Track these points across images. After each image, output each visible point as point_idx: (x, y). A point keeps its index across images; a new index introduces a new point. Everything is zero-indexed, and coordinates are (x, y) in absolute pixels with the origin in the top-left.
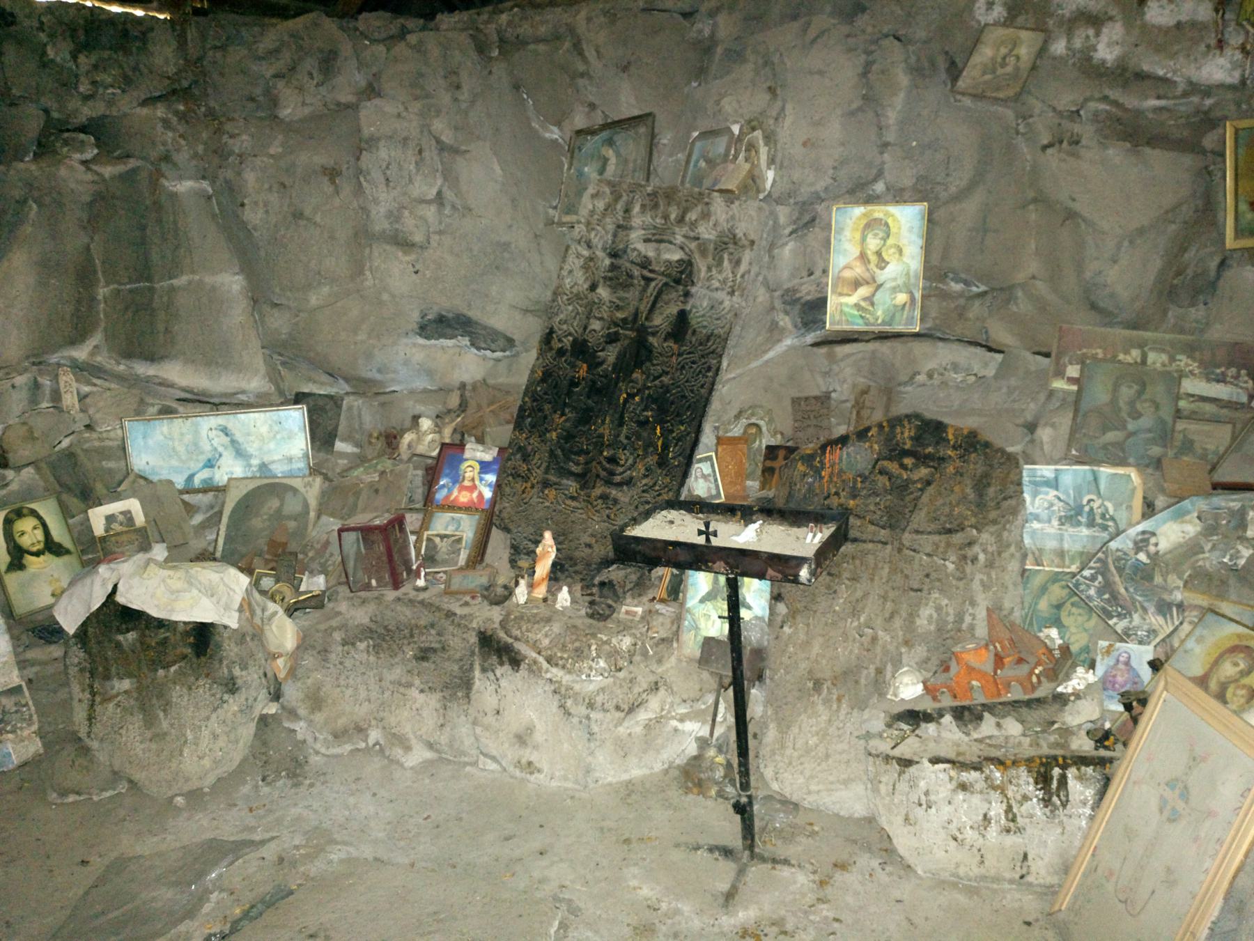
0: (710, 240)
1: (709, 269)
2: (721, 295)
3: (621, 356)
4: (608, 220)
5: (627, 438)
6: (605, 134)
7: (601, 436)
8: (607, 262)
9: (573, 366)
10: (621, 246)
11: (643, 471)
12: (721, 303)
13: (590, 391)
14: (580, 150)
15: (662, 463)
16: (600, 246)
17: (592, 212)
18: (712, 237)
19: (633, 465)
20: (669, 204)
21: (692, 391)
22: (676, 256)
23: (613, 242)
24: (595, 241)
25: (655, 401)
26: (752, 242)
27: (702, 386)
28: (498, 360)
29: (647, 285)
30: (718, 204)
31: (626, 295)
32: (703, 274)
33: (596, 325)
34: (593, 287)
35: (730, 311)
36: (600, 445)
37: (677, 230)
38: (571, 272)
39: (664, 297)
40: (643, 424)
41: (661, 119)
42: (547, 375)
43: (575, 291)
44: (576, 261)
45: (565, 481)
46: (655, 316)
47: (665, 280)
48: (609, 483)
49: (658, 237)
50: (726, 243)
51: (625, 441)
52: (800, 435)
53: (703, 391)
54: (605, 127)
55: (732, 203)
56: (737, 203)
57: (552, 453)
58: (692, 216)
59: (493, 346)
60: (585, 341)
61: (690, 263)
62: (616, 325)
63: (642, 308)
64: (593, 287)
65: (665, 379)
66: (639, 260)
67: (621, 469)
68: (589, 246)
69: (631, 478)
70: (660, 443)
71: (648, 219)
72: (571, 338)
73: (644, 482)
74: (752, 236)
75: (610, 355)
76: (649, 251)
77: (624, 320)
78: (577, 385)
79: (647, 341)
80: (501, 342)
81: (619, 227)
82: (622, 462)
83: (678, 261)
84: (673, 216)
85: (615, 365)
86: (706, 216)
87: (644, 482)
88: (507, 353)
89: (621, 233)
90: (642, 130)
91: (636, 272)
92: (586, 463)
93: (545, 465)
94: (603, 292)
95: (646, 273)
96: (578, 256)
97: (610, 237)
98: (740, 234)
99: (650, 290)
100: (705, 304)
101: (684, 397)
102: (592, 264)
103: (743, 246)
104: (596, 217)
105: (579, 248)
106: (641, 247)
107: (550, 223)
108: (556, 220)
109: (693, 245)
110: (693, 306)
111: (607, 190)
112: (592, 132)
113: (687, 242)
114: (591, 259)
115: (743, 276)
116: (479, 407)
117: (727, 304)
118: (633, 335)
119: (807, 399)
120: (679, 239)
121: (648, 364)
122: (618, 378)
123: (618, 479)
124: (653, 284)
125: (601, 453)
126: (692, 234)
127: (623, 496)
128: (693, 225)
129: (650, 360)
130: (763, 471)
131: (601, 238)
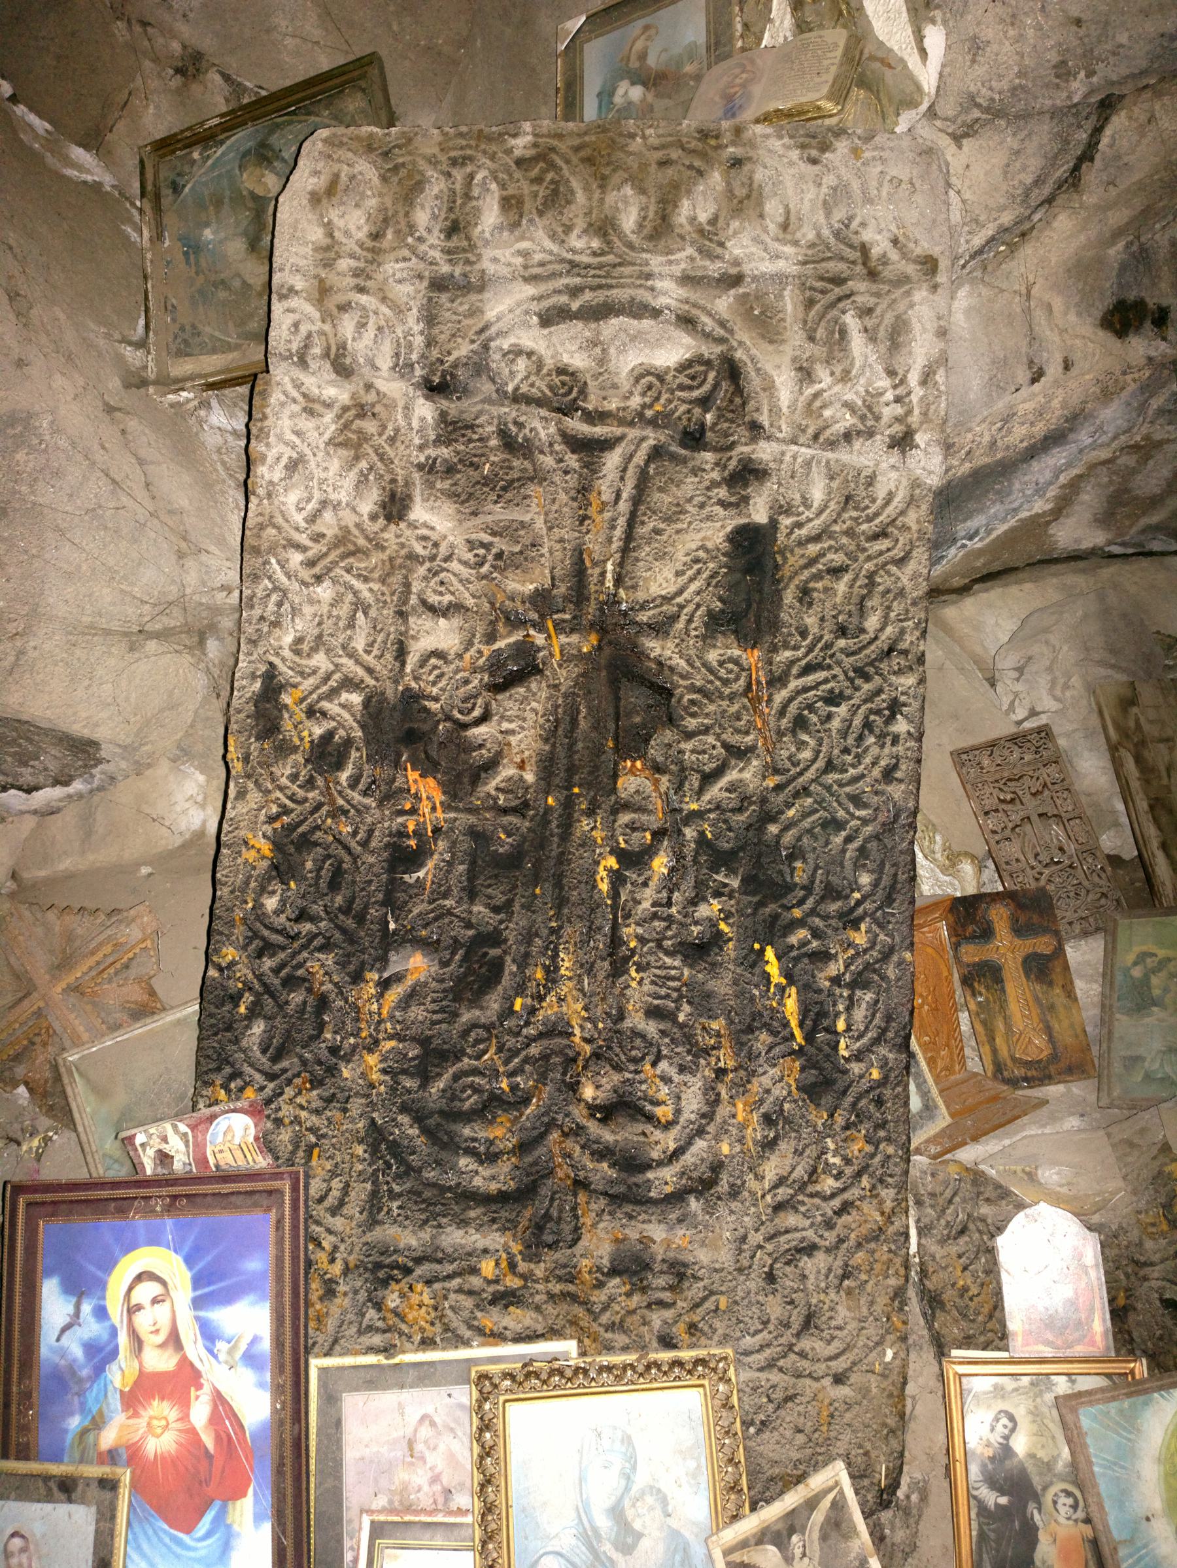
0: (780, 279)
1: (805, 374)
2: (867, 455)
3: (560, 728)
4: (392, 268)
5: (653, 1013)
6: (243, 138)
7: (558, 1029)
8: (425, 410)
9: (390, 795)
10: (463, 350)
11: (756, 1131)
12: (871, 481)
13: (472, 875)
14: (176, 189)
15: (822, 1081)
16: (385, 362)
17: (328, 253)
18: (781, 265)
19: (708, 1116)
20: (603, 183)
21: (856, 800)
22: (671, 351)
23: (430, 343)
24: (361, 346)
25: (722, 860)
26: (930, 265)
27: (888, 774)
28: (51, 811)
29: (592, 468)
30: (778, 163)
31: (516, 515)
32: (785, 394)
33: (439, 635)
34: (394, 507)
35: (911, 501)
36: (561, 1064)
37: (656, 262)
38: (293, 466)
39: (661, 500)
40: (700, 951)
41: (399, 75)
42: (290, 846)
43: (328, 523)
44: (307, 424)
45: (454, 1237)
46: (640, 570)
47: (652, 438)
48: (628, 1198)
49: (589, 299)
50: (838, 281)
51: (651, 1028)
52: (1012, 849)
53: (896, 791)
54: (234, 120)
55: (825, 147)
56: (842, 146)
57: (376, 1138)
58: (697, 207)
59: (27, 775)
60: (411, 698)
61: (732, 371)
62: (514, 622)
63: (594, 544)
64: (394, 507)
65: (747, 774)
66: (540, 386)
67: (670, 1140)
68: (343, 369)
69: (717, 1167)
70: (791, 1005)
71: (539, 241)
72: (356, 699)
73: (772, 1168)
74: (924, 246)
75: (516, 732)
76: (567, 347)
77: (541, 600)
78: (414, 859)
79: (642, 655)
80: (52, 759)
81: (439, 285)
82: (664, 1112)
83: (683, 367)
84: (629, 221)
85: (547, 765)
86: (744, 202)
87: (772, 1168)
88: (77, 786)
89: (450, 308)
90: (353, 103)
91: (541, 427)
92: (523, 1148)
93: (361, 1191)
94: (434, 517)
95: (577, 425)
96: (312, 407)
97: (414, 323)
98: (880, 245)
99: (605, 487)
100: (817, 495)
101: (835, 824)
102: (370, 426)
103: (903, 280)
104: (344, 264)
105: (310, 382)
106: (531, 338)
107: (136, 381)
108: (151, 374)
109: (723, 304)
110: (781, 509)
111: (367, 169)
112: (206, 138)
113: (694, 296)
114: (363, 411)
115: (926, 379)
116: (25, 987)
117: (888, 481)
118: (587, 644)
119: (992, 745)
120: (669, 293)
121: (668, 735)
122: (568, 804)
123: (665, 1179)
124: (612, 460)
125: (574, 1087)
126: (714, 268)
127: (708, 1242)
128: (709, 237)
129: (672, 721)
130: (966, 981)
131: (383, 337)
